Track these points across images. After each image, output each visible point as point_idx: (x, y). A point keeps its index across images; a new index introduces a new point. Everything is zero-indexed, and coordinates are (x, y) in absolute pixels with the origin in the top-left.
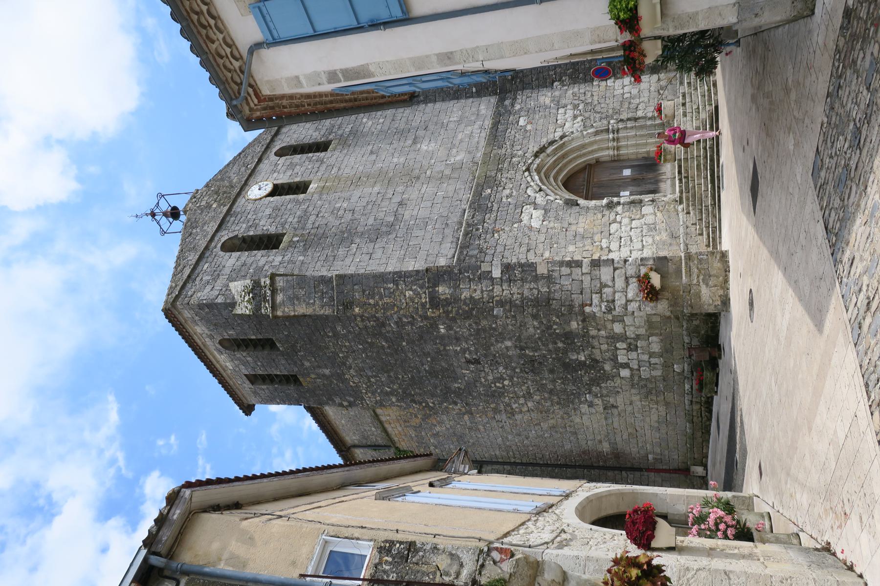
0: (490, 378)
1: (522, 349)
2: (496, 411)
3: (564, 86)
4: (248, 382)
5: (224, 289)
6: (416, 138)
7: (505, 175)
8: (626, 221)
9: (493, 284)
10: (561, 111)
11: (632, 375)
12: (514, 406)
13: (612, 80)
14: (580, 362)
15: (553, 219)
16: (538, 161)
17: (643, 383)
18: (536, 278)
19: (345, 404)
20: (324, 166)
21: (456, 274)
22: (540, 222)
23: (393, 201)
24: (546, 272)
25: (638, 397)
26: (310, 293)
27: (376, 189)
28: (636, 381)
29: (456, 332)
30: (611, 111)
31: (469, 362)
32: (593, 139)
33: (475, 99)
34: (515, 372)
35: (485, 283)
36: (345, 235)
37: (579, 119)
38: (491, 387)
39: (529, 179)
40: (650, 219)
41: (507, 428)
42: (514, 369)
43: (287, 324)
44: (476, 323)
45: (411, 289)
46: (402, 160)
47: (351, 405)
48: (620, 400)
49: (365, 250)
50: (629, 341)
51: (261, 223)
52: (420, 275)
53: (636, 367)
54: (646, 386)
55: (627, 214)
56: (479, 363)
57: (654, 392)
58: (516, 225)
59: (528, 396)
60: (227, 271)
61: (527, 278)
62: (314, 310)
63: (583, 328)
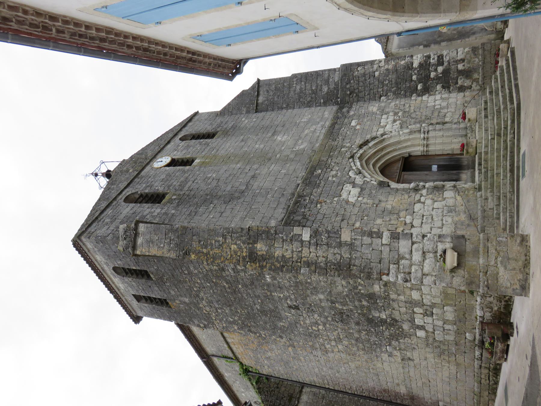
0: (308, 322)
1: (333, 302)
2: (313, 347)
3: (389, 99)
4: (135, 300)
6: (275, 132)
7: (333, 160)
9: (302, 246)
10: (384, 116)
11: (427, 337)
12: (328, 346)
13: (427, 95)
14: (382, 319)
16: (361, 151)
17: (436, 344)
18: (340, 245)
19: (202, 325)
20: (209, 148)
21: (272, 235)
23: (248, 175)
24: (349, 240)
25: (432, 355)
26: (161, 239)
27: (239, 165)
28: (430, 341)
29: (279, 282)
30: (423, 118)
31: (290, 307)
32: (407, 137)
33: (322, 108)
34: (327, 320)
35: (296, 244)
36: (208, 197)
37: (398, 122)
38: (308, 329)
39: (352, 164)
40: (451, 202)
41: (322, 362)
42: (326, 318)
43: (156, 260)
44: (294, 276)
45: (236, 244)
46: (262, 146)
47: (205, 327)
48: (415, 355)
50: (425, 307)
51: (156, 185)
53: (431, 330)
54: (439, 347)
55: (431, 196)
56: (299, 309)
57: (446, 353)
58: (336, 199)
59: (339, 340)
60: (122, 216)
61: (331, 244)
62: (163, 253)
63: (385, 291)
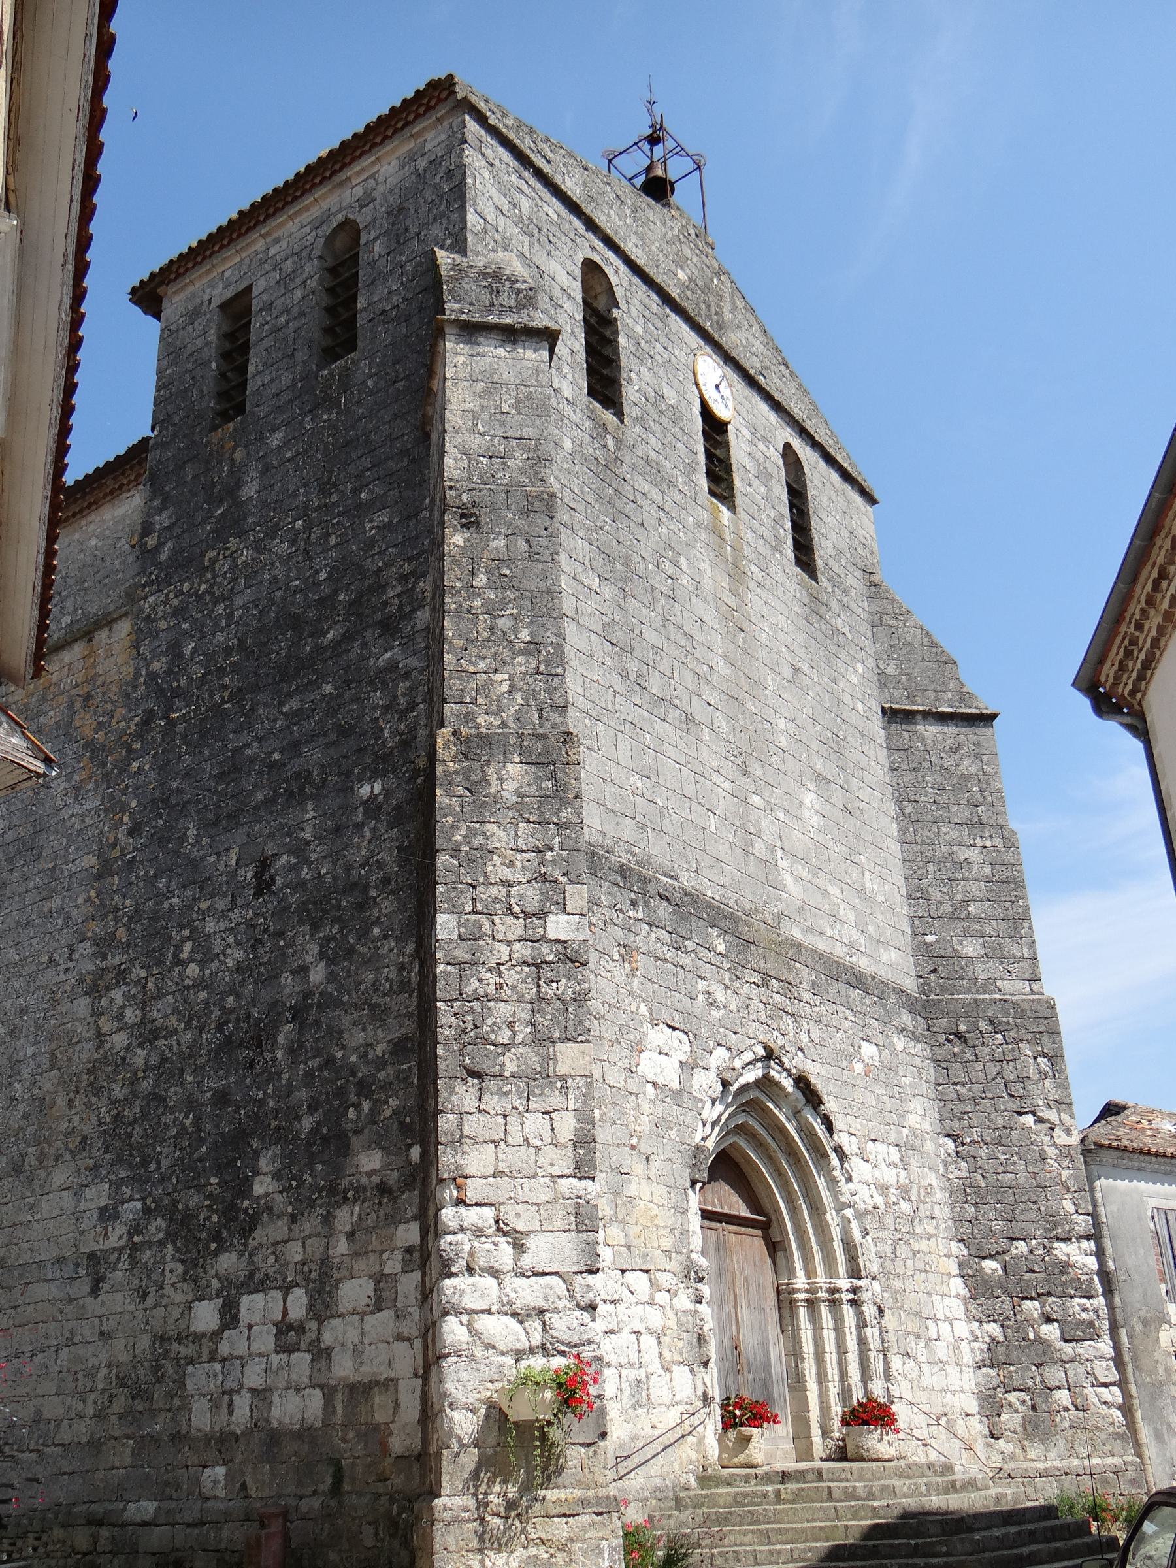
0: (211, 926)
1: (298, 1013)
2: (104, 945)
3: (945, 1165)
4: (229, 294)
5: (498, 237)
6: (829, 782)
7: (755, 992)
8: (655, 1319)
9: (526, 915)
10: (894, 1155)
11: (198, 1337)
12: (117, 995)
13: (964, 1292)
14: (248, 1182)
15: (659, 1112)
16: (787, 1084)
17: (169, 1369)
18: (542, 1040)
19: (151, 541)
20: (766, 551)
21: (557, 813)
22: (651, 1078)
23: (695, 699)
24: (562, 1069)
25: (124, 1357)
26: (504, 424)
27: (720, 664)
28: (173, 1352)
29: (359, 827)
30: (898, 1284)
31: (264, 864)
32: (836, 1233)
33: (909, 940)
34: (224, 995)
35: (531, 895)
36: (618, 566)
37: (879, 1200)
38: (182, 927)
39: (748, 1056)
40: (659, 1389)
41: (51, 977)
42: (233, 991)
43: (400, 385)
44: (386, 881)
45: (512, 689)
46: (783, 741)
47: (146, 555)
48: (117, 1300)
49: (585, 607)
50: (312, 1325)
51: (644, 371)
52: (554, 716)
53: (224, 1349)
54: (160, 1380)
55: (672, 1323)
56: (257, 895)
57: (139, 1405)
58: (643, 1009)
59: (148, 1034)
60: (540, 258)
61: (542, 1012)
62: (457, 431)
63: (360, 1190)
